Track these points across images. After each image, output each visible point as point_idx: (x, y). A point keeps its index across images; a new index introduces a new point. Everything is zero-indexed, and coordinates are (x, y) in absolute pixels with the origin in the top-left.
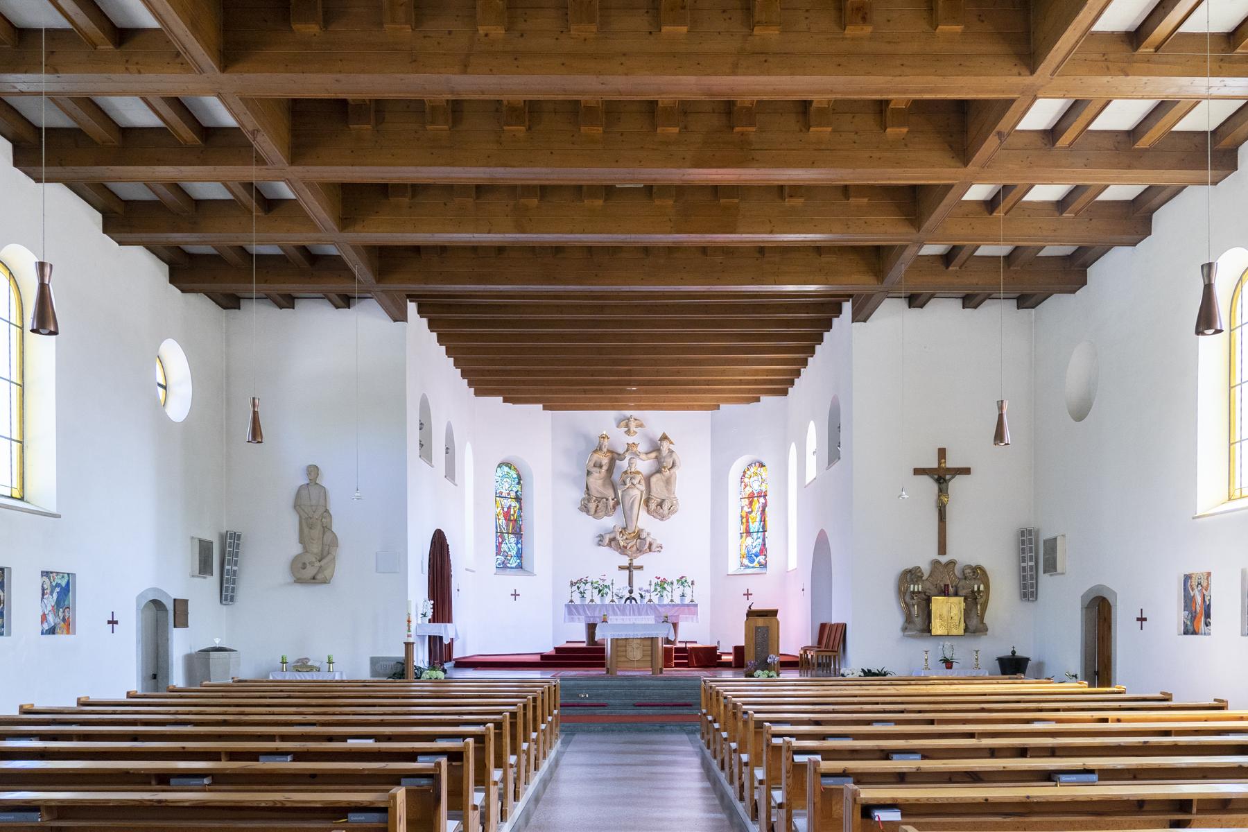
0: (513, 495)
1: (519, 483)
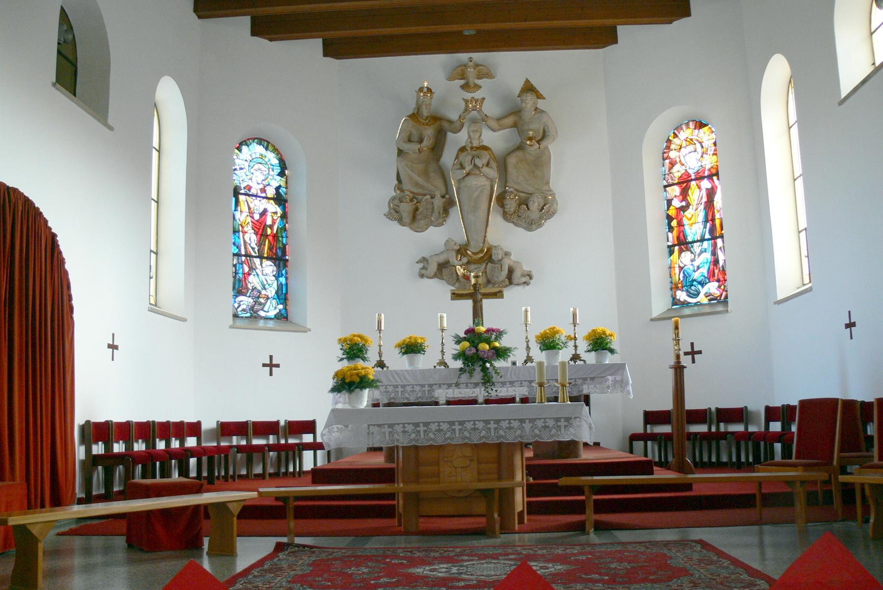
0: (271, 192)
1: (282, 174)
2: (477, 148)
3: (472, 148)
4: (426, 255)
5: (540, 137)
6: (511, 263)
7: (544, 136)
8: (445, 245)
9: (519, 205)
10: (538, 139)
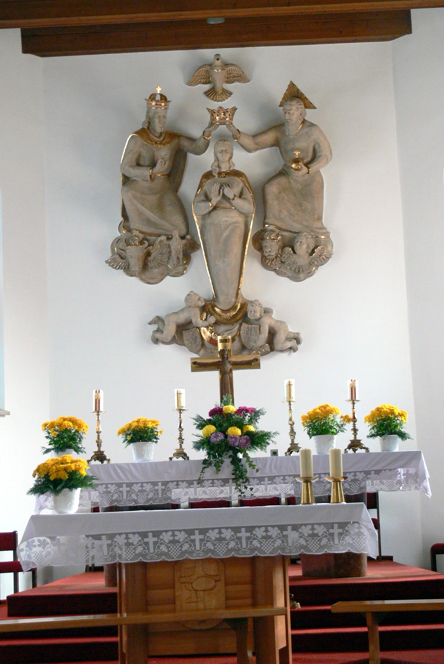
2: (227, 174)
3: (220, 174)
4: (162, 314)
5: (309, 159)
6: (273, 323)
7: (315, 157)
8: (186, 300)
9: (283, 247)
10: (305, 161)
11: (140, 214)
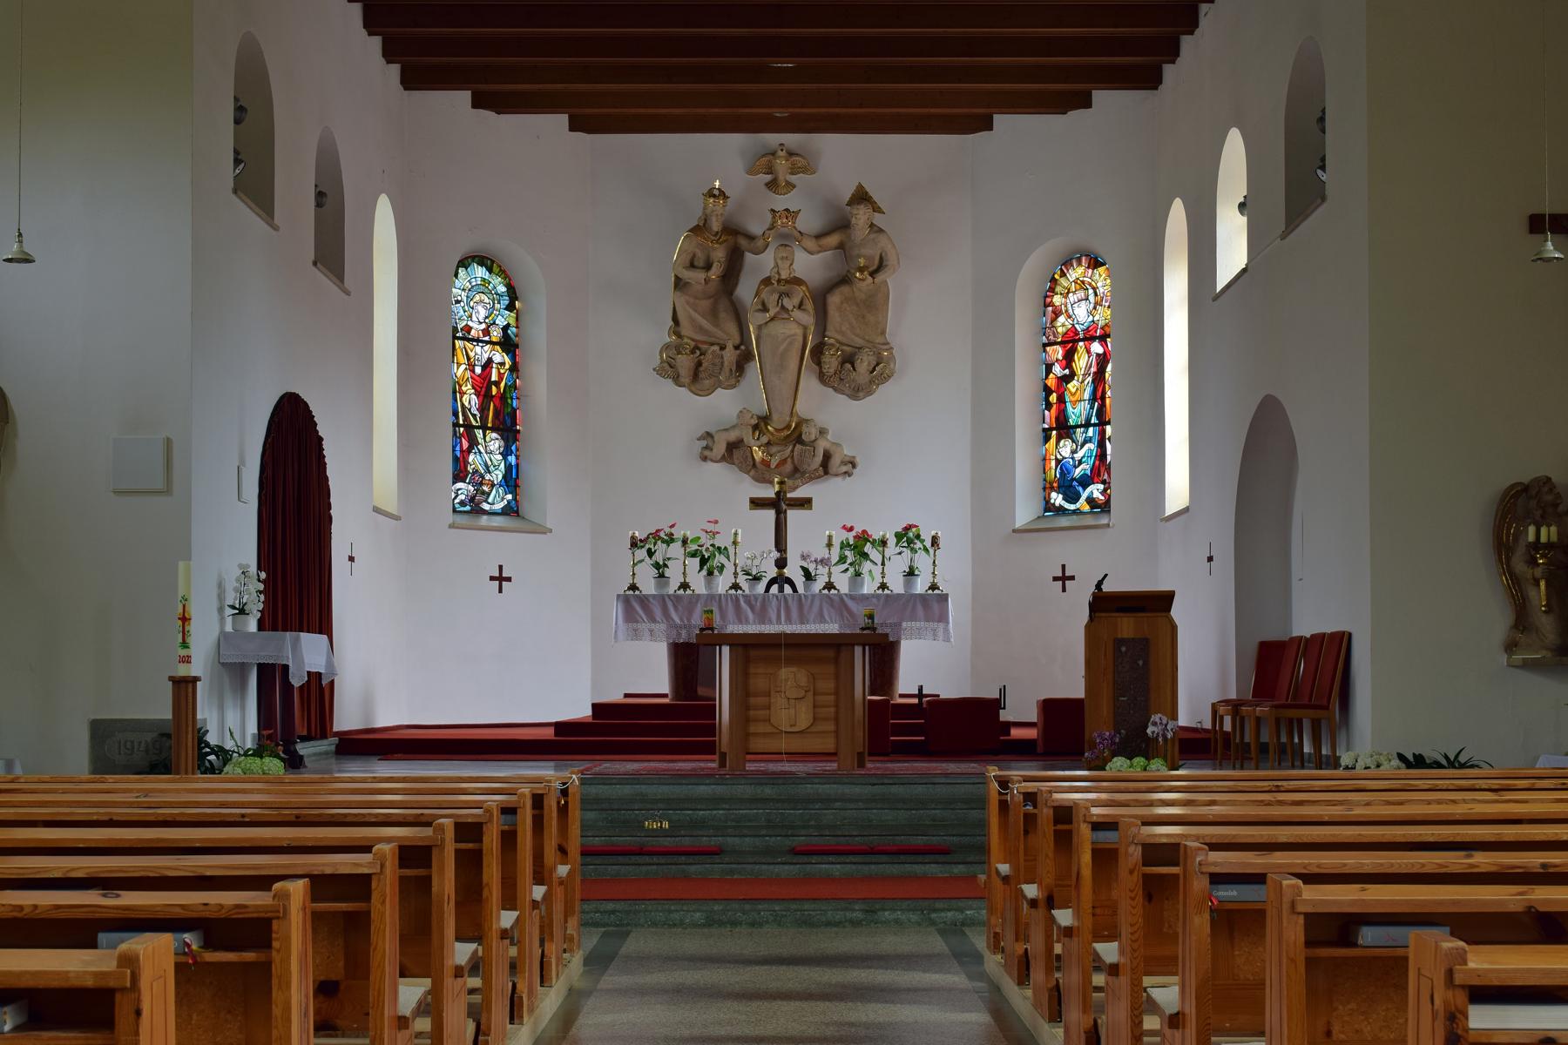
2: (787, 282)
3: (779, 281)
4: (712, 430)
7: (881, 266)
11: (692, 320)
